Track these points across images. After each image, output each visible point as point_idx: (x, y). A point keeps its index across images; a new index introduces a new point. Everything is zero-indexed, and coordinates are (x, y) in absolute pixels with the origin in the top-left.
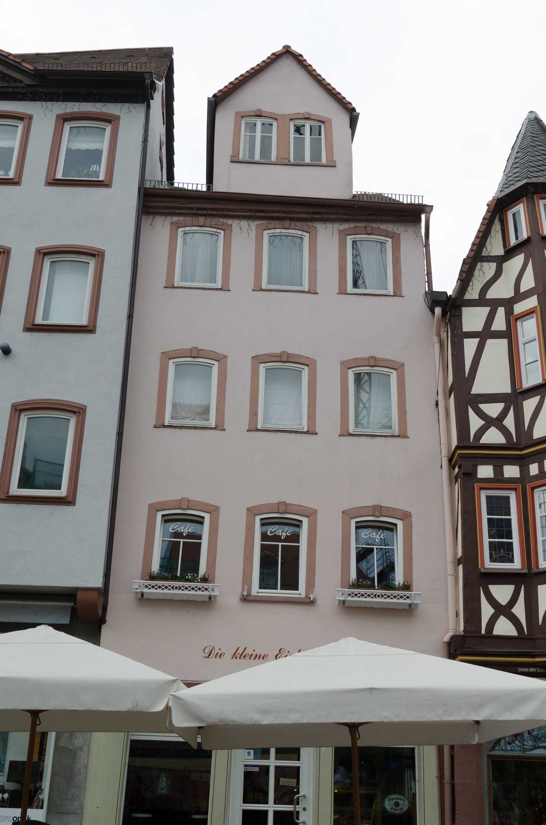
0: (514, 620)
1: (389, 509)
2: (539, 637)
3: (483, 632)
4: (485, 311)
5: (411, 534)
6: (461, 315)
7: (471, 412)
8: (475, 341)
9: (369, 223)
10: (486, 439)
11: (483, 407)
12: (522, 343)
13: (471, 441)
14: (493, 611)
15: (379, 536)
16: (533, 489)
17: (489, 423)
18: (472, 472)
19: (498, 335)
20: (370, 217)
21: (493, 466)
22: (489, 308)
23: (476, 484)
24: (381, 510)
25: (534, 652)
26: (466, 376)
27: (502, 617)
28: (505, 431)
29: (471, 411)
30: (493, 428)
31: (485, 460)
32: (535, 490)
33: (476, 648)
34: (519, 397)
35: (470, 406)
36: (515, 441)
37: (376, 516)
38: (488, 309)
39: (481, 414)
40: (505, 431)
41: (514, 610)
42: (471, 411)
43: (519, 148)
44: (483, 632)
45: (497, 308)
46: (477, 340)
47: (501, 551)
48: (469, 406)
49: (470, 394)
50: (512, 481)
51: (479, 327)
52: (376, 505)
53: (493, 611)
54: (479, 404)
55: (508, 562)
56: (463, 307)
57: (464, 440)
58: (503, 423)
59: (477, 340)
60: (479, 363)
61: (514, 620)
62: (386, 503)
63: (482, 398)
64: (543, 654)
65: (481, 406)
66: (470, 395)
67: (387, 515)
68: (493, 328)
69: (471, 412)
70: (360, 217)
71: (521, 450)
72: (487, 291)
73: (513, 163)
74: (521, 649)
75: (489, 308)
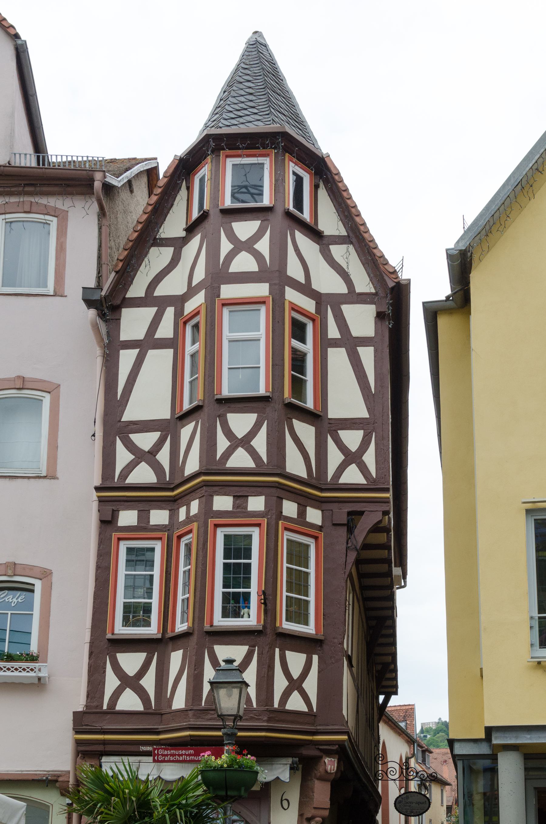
0: (142, 693)
1: (25, 566)
2: (165, 712)
3: (105, 707)
4: (150, 312)
5: (50, 596)
6: (120, 319)
7: (119, 445)
8: (135, 352)
9: (24, 196)
10: (133, 479)
11: (134, 437)
12: (188, 354)
13: (116, 480)
14: (118, 683)
15: (17, 599)
16: (179, 537)
17: (139, 458)
18: (110, 519)
19: (162, 344)
20: (27, 189)
21: (139, 511)
22: (156, 308)
23: (113, 534)
24: (14, 568)
25: (157, 729)
26: (118, 399)
27: (128, 689)
28: (157, 467)
29: (119, 443)
30: (143, 463)
31: (129, 503)
32: (182, 539)
33: (95, 725)
34: (179, 423)
35: (119, 437)
36: (168, 479)
37: (8, 576)
38: (154, 310)
39: (131, 446)
40: (157, 467)
41: (142, 682)
42: (119, 443)
43: (227, 86)
44: (105, 707)
45: (165, 310)
46: (136, 351)
47: (140, 613)
48: (117, 437)
49: (120, 421)
50: (158, 529)
51: (140, 335)
52: (8, 563)
53: (118, 683)
54: (130, 434)
55: (144, 626)
56: (123, 308)
57: (107, 480)
58: (156, 457)
59: (136, 351)
60: (135, 381)
61: (142, 693)
62: (22, 559)
63: (135, 426)
64: (165, 731)
65: (133, 436)
66: (119, 424)
67: (22, 574)
68: (157, 336)
69: (119, 445)
70: (13, 189)
71: (172, 490)
72: (157, 286)
73: (216, 108)
74: (145, 726)
75: (156, 308)
